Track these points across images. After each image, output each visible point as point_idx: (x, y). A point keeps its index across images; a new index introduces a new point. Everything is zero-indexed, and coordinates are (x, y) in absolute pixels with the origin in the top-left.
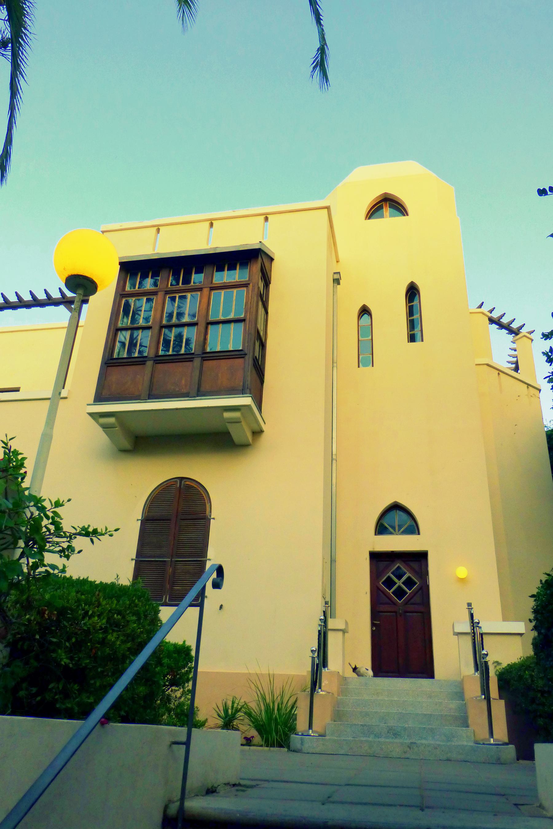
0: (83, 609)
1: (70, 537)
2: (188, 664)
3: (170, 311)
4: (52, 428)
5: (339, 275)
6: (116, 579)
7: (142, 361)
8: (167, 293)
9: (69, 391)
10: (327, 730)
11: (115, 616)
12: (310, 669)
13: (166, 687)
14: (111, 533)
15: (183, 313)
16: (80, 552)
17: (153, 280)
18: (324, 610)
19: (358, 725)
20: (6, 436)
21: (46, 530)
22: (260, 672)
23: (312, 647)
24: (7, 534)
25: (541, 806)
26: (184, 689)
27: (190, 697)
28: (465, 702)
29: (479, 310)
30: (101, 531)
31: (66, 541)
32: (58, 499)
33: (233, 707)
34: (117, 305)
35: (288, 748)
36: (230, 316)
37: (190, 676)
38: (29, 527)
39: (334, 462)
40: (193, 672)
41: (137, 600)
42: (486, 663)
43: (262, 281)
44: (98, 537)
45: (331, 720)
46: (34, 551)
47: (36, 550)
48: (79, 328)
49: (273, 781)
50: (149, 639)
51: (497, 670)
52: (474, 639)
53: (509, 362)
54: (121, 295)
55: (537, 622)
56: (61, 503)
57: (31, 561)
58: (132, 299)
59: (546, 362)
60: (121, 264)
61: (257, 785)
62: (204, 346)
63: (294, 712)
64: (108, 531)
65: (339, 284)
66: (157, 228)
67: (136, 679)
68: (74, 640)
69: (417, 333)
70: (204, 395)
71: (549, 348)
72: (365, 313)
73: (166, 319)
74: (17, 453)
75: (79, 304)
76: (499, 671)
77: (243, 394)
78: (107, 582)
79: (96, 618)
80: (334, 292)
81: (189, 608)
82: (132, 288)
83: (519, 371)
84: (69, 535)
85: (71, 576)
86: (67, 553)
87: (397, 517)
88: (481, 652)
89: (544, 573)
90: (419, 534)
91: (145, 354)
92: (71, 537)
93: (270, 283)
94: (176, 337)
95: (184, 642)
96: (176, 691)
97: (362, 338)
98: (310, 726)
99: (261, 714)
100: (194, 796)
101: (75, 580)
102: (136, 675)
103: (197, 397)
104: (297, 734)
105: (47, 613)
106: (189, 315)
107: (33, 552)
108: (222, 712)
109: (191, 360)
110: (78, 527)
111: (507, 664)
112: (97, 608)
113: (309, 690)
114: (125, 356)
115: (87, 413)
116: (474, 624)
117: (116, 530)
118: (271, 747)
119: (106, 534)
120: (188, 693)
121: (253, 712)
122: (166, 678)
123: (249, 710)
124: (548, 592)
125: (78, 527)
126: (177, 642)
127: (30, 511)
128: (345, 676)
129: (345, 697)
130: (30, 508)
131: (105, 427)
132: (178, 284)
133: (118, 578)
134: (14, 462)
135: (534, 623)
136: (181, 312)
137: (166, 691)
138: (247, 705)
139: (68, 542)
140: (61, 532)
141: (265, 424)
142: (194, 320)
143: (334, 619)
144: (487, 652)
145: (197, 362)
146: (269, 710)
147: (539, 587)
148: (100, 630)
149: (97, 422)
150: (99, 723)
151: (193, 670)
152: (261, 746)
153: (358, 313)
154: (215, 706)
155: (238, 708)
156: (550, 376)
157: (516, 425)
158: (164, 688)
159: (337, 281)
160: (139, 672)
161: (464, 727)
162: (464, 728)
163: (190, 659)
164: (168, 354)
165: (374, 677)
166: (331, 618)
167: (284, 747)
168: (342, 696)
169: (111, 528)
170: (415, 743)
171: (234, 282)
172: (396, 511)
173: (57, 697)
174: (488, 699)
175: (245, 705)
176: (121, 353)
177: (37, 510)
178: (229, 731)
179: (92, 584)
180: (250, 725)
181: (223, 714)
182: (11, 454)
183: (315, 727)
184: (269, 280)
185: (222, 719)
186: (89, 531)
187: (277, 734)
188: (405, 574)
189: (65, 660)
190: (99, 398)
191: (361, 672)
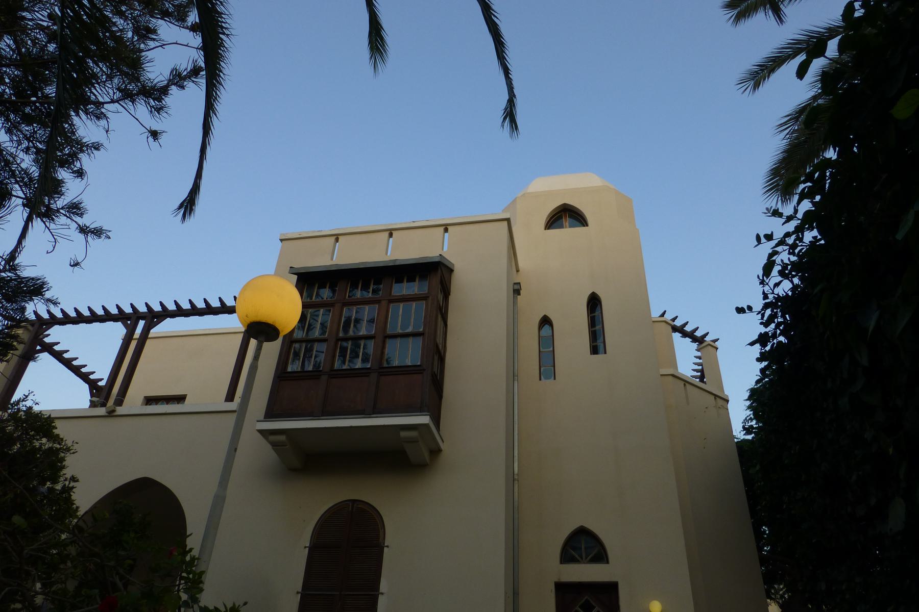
5: (519, 286)
72: (547, 324)
82: (309, 299)
90: (608, 562)
93: (449, 294)
131: (274, 445)
141: (443, 442)
149: (267, 439)
159: (517, 292)
171: (413, 295)
190: (270, 414)
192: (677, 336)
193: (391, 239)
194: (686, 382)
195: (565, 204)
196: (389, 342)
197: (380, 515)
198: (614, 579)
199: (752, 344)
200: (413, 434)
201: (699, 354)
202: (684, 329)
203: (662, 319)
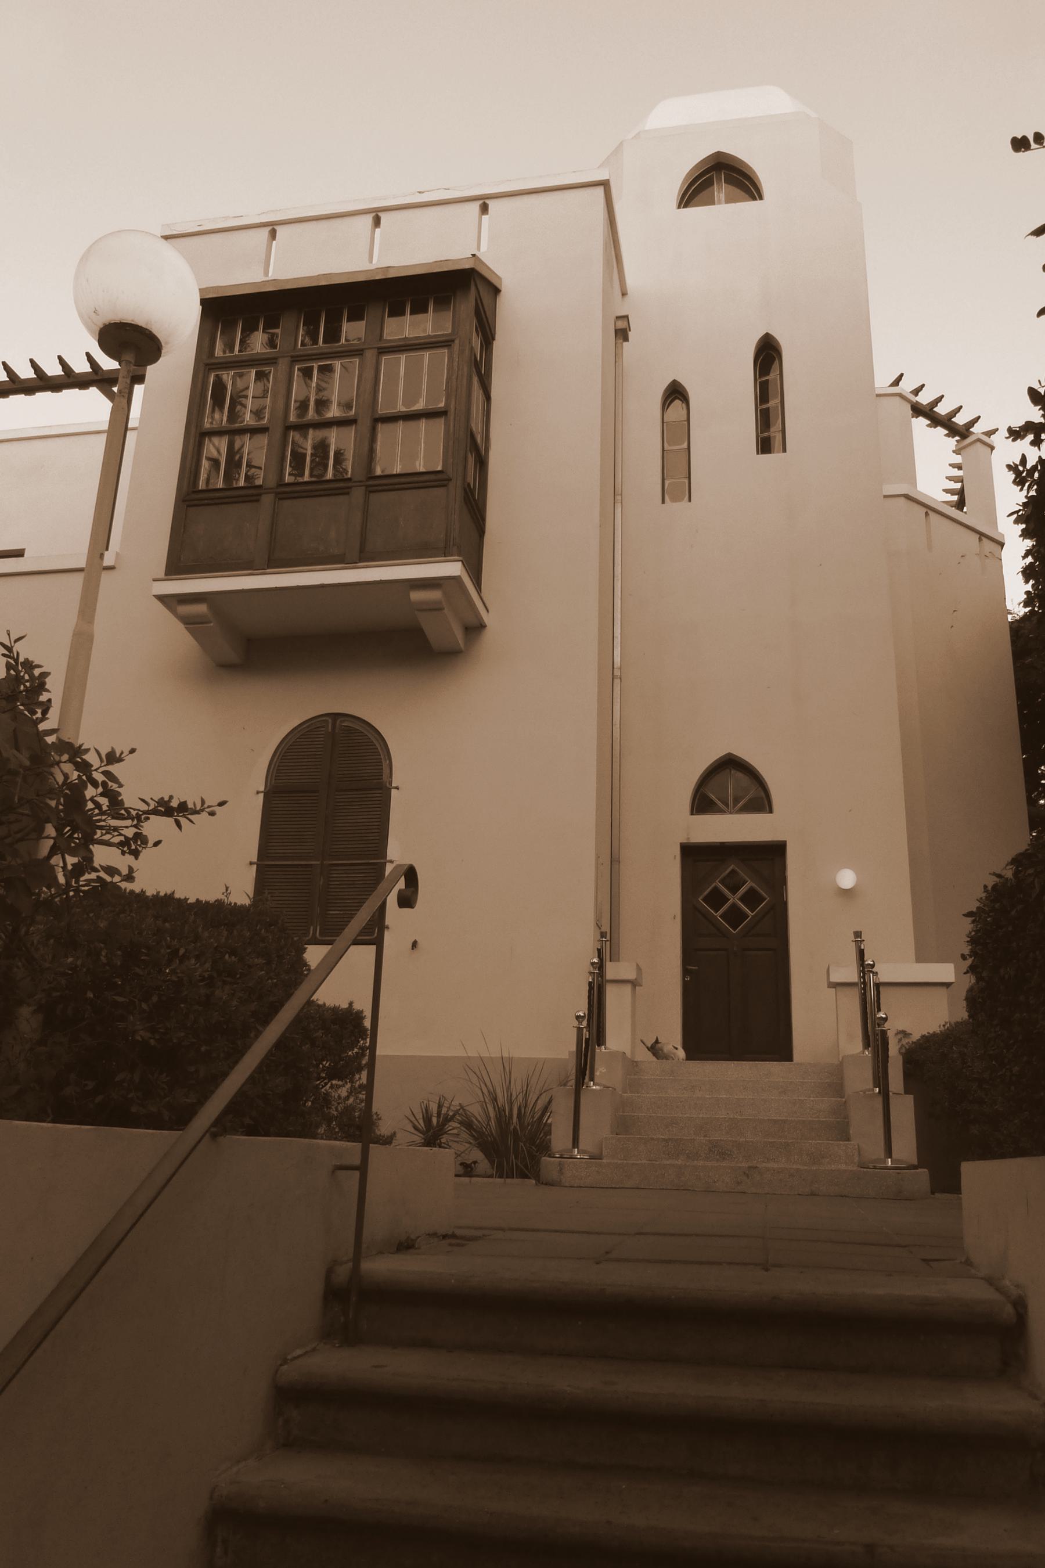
0: (169, 947)
2: (359, 1042)
3: (301, 398)
4: (91, 622)
6: (225, 894)
7: (252, 494)
8: (295, 360)
10: (604, 1149)
11: (227, 956)
12: (574, 1048)
13: (322, 1082)
14: (211, 809)
16: (157, 844)
17: (266, 336)
18: (599, 948)
19: (658, 1139)
20: (9, 635)
22: (487, 1055)
23: (579, 1011)
24: (23, 814)
25: (968, 1263)
26: (353, 1082)
27: (364, 1097)
28: (844, 1100)
30: (193, 807)
31: (131, 826)
32: (112, 748)
33: (439, 1113)
35: (535, 1180)
36: (417, 405)
37: (364, 1062)
38: (62, 800)
39: (617, 681)
40: (368, 1054)
41: (263, 930)
42: (884, 1033)
44: (189, 816)
45: (612, 1133)
46: (75, 843)
47: (77, 841)
48: (129, 433)
49: (512, 1229)
50: (289, 996)
51: (902, 1045)
53: (947, 491)
54: (207, 365)
55: (975, 958)
56: (118, 755)
57: (71, 860)
58: (228, 374)
59: (1013, 485)
60: (204, 302)
61: (484, 1235)
62: (371, 464)
64: (206, 806)
66: (270, 228)
68: (155, 999)
69: (775, 436)
70: (373, 559)
71: (1020, 457)
73: (295, 412)
74: (31, 665)
75: (128, 381)
76: (905, 1048)
77: (445, 556)
78: (208, 899)
79: (193, 961)
82: (227, 351)
83: (965, 509)
84: (137, 814)
85: (142, 890)
86: (133, 847)
87: (734, 781)
88: (875, 1015)
89: (990, 874)
90: (771, 811)
92: (139, 818)
93: (494, 339)
94: (315, 447)
95: (351, 1004)
96: (339, 1087)
97: (670, 445)
98: (575, 1143)
99: (488, 1123)
101: (151, 897)
102: (266, 1057)
103: (360, 562)
104: (552, 1156)
105: (103, 954)
106: (339, 404)
107: (73, 845)
108: (421, 1121)
109: (345, 492)
110: (152, 799)
112: (193, 945)
113: (573, 1082)
114: (220, 485)
115: (154, 596)
116: (865, 968)
117: (221, 804)
118: (507, 1177)
119: (202, 810)
120: (359, 1090)
121: (476, 1122)
122: (321, 1066)
123: (467, 1118)
124: (997, 906)
125: (152, 799)
126: (337, 1005)
127: (62, 772)
128: (636, 1060)
131: (188, 621)
132: (315, 341)
133: (228, 892)
134: (27, 681)
135: (969, 961)
138: (464, 1110)
139: (136, 826)
141: (488, 611)
142: (348, 415)
143: (617, 963)
144: (886, 1014)
145: (358, 493)
146: (503, 1119)
147: (981, 898)
148: (203, 980)
150: (208, 1135)
151: (368, 1051)
152: (491, 1176)
154: (409, 1114)
156: (1020, 510)
157: (955, 611)
158: (318, 1082)
162: (841, 1142)
163: (362, 1032)
164: (300, 480)
165: (687, 1059)
166: (610, 961)
167: (530, 1178)
168: (631, 1092)
169: (212, 800)
170: (756, 1167)
171: (425, 337)
172: (731, 772)
173: (130, 1096)
174: (885, 1094)
175: (461, 1110)
176: (212, 481)
177: (76, 770)
178: (434, 1149)
179: (182, 903)
180: (470, 1143)
181: (423, 1125)
182: (20, 668)
183: (582, 1145)
185: (421, 1133)
186: (172, 807)
188: (745, 882)
189: (142, 1033)
190: (176, 567)
191: (665, 1051)
197: (384, 740)
200: (434, 595)
202: (935, 409)
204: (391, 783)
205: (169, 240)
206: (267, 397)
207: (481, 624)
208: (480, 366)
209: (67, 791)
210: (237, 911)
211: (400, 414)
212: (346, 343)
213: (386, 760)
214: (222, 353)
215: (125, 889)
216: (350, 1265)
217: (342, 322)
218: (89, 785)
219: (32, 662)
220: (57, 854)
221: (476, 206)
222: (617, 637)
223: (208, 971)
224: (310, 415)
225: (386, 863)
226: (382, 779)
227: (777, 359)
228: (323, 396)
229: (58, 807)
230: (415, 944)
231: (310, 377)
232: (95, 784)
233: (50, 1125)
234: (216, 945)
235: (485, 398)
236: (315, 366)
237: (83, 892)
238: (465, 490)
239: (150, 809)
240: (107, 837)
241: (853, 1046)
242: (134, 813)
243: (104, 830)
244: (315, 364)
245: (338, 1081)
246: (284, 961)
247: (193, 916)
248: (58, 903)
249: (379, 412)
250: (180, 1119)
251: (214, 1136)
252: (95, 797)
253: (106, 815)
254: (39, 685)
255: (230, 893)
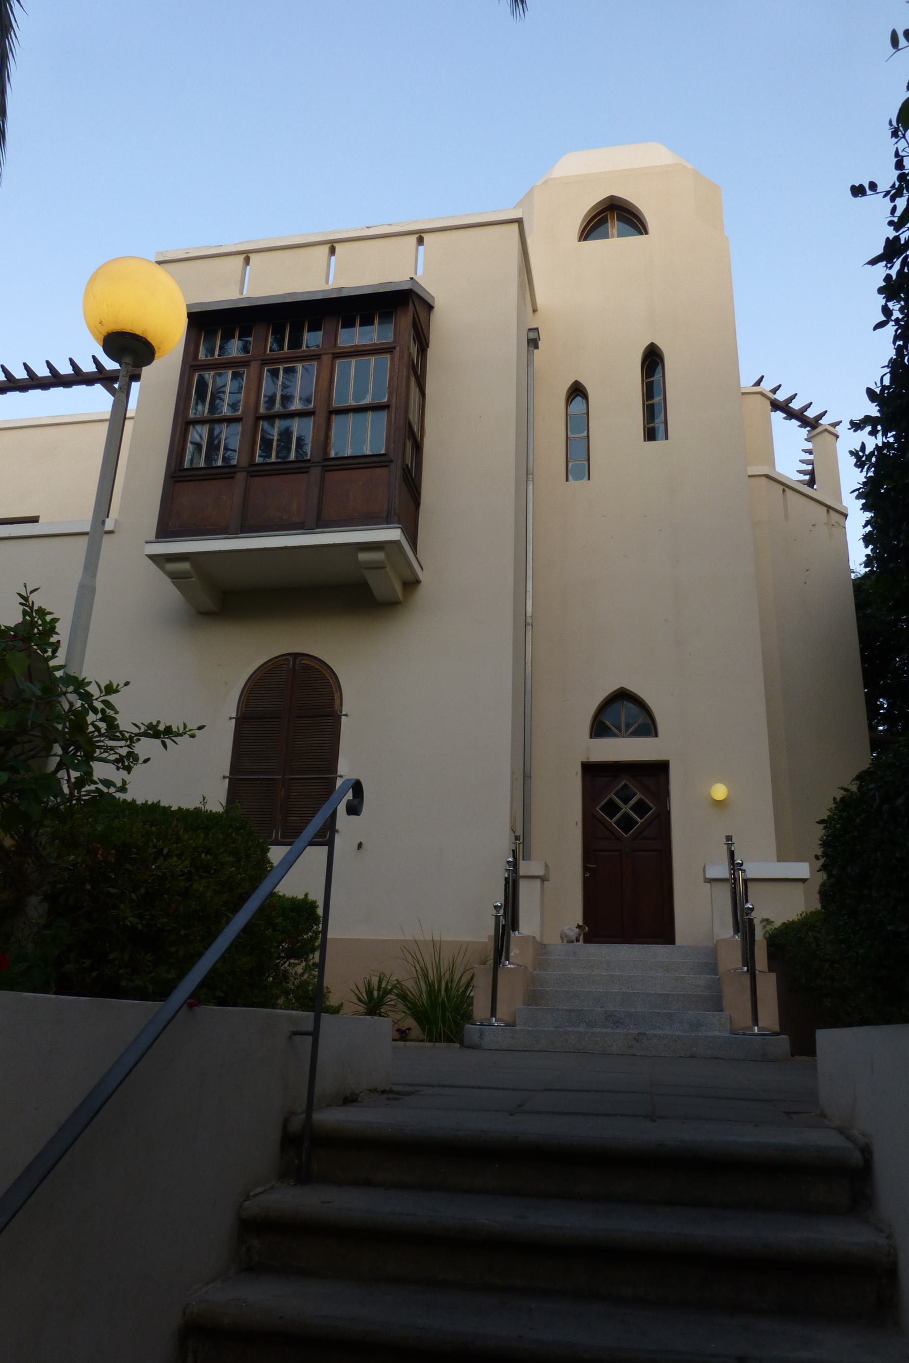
0: (155, 847)
1: (131, 739)
2: (313, 927)
3: (270, 394)
4: (94, 576)
5: (536, 334)
7: (228, 472)
8: (264, 362)
9: (116, 520)
11: (203, 855)
12: (492, 933)
14: (192, 732)
15: (292, 396)
16: (146, 761)
17: (241, 343)
18: (514, 849)
20: (25, 587)
21: (94, 730)
23: (496, 902)
24: (35, 736)
25: (823, 1115)
27: (317, 973)
28: (718, 976)
29: (757, 389)
31: (125, 746)
32: (110, 682)
34: (186, 384)
37: (317, 944)
38: (67, 724)
39: (529, 627)
40: (320, 937)
41: (234, 834)
42: (751, 921)
43: (415, 344)
44: (173, 738)
46: (78, 760)
47: (80, 758)
48: (127, 422)
49: (439, 1086)
50: (255, 888)
51: (766, 931)
52: (735, 888)
53: (800, 472)
54: (191, 366)
55: (826, 859)
56: (114, 687)
57: (74, 774)
58: (209, 374)
59: (854, 467)
60: (190, 315)
63: (470, 994)
64: (187, 729)
65: (537, 347)
66: (245, 255)
67: (236, 946)
68: (142, 890)
69: (659, 427)
71: (860, 445)
73: (264, 405)
74: (44, 612)
75: (127, 379)
76: (769, 933)
77: (387, 524)
78: (188, 808)
79: (175, 859)
80: (530, 361)
81: (308, 847)
82: (209, 355)
83: (815, 487)
84: (130, 736)
85: (133, 800)
86: (126, 763)
87: (626, 710)
88: (744, 905)
90: (656, 736)
91: (234, 462)
92: (132, 740)
93: (428, 346)
94: (280, 434)
95: (306, 895)
96: (296, 965)
97: (572, 434)
98: (493, 1012)
99: (420, 995)
100: (326, 1106)
104: (474, 1023)
105: (100, 852)
106: (301, 399)
107: (76, 761)
109: (305, 471)
110: (142, 723)
111: (781, 923)
112: (175, 845)
113: (491, 962)
115: (146, 555)
116: (735, 866)
117: (200, 728)
118: (436, 1042)
119: (185, 733)
120: (313, 968)
121: (410, 995)
122: (281, 947)
123: (402, 991)
124: (845, 814)
125: (142, 723)
126: (295, 896)
127: (68, 700)
128: (544, 943)
129: (545, 972)
130: (68, 695)
131: (174, 577)
132: (281, 348)
133: (205, 801)
134: (40, 625)
135: (822, 861)
136: (288, 394)
137: (282, 966)
138: (401, 985)
139: (129, 746)
140: (117, 732)
141: (422, 569)
142: (308, 407)
143: (529, 862)
144: (752, 905)
145: (316, 472)
146: (432, 992)
147: (831, 808)
148: (181, 875)
149: (162, 568)
151: (320, 934)
152: (422, 1041)
153: (567, 394)
154: (354, 989)
155: (387, 989)
156: (861, 488)
157: (807, 570)
158: (278, 961)
159: (533, 343)
160: (238, 937)
161: (716, 1011)
162: (716, 1013)
163: (316, 920)
164: (268, 461)
166: (523, 860)
167: (454, 1042)
168: (540, 970)
170: (645, 1034)
172: (623, 703)
173: (121, 971)
175: (398, 985)
176: (195, 461)
177: (80, 699)
178: (375, 1017)
179: (166, 810)
180: (405, 1012)
181: (366, 999)
182: (34, 615)
183: (499, 1015)
184: (426, 342)
185: (365, 1004)
186: (159, 730)
187: (444, 1025)
188: (635, 795)
189: (131, 919)
190: (165, 531)
192: (778, 417)
193: (333, 258)
194: (786, 486)
195: (612, 198)
196: (336, 421)
198: (663, 757)
199: (874, 262)
201: (809, 446)
203: (757, 389)
204: (341, 711)
205: (161, 265)
206: (241, 393)
207: (417, 580)
208: (416, 368)
209: (72, 717)
210: (212, 816)
211: (351, 407)
212: (307, 349)
213: (337, 693)
214: (204, 356)
215: (119, 799)
216: (304, 1116)
217: (303, 332)
218: (90, 712)
219: (45, 610)
220: (62, 769)
221: (413, 239)
222: (529, 592)
223: (188, 868)
224: (276, 407)
225: (336, 777)
226: (333, 708)
227: (660, 364)
228: (287, 392)
229: (64, 730)
230: (360, 846)
231: (277, 377)
232: (95, 711)
233: (54, 996)
234: (194, 845)
235: (420, 395)
236: (281, 367)
237: (84, 800)
238: (404, 469)
239: (141, 732)
240: (104, 755)
241: (725, 931)
242: (127, 735)
243: (102, 749)
244: (280, 367)
245: (295, 960)
246: (251, 859)
247: (176, 821)
248: (63, 810)
249: (334, 406)
250: (163, 992)
251: (191, 1006)
252: (95, 721)
253: (103, 737)
254: (51, 629)
255: (206, 802)
